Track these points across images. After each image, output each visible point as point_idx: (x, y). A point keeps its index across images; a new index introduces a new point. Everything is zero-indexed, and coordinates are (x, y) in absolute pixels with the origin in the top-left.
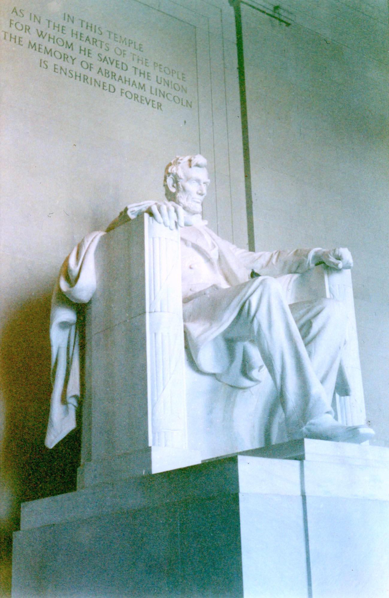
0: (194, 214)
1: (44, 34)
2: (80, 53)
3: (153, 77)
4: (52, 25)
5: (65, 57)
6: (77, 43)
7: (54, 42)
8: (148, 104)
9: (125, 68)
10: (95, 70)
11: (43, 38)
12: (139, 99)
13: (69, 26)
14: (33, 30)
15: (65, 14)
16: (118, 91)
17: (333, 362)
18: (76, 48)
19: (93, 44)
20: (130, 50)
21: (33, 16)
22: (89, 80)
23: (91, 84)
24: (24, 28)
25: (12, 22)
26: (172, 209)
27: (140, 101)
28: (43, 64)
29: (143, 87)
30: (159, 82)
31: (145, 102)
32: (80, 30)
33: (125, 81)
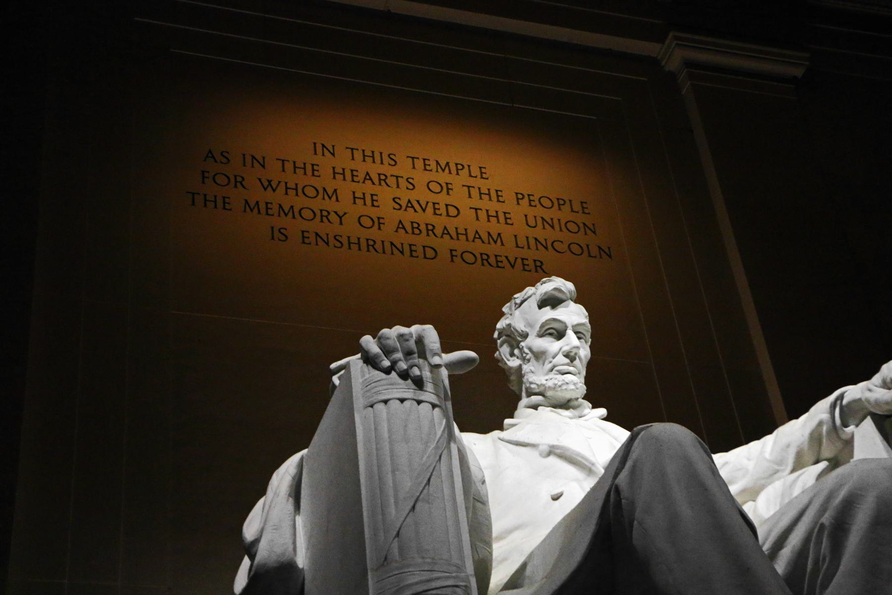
1: (274, 184)
2: (355, 203)
5: (325, 216)
6: (345, 189)
7: (297, 195)
8: (513, 267)
11: (274, 191)
12: (492, 260)
13: (326, 163)
15: (315, 144)
16: (444, 254)
19: (380, 184)
20: (458, 181)
21: (249, 160)
22: (378, 246)
23: (384, 252)
24: (233, 180)
25: (206, 175)
27: (495, 265)
30: (532, 223)
32: (349, 165)
33: (458, 234)
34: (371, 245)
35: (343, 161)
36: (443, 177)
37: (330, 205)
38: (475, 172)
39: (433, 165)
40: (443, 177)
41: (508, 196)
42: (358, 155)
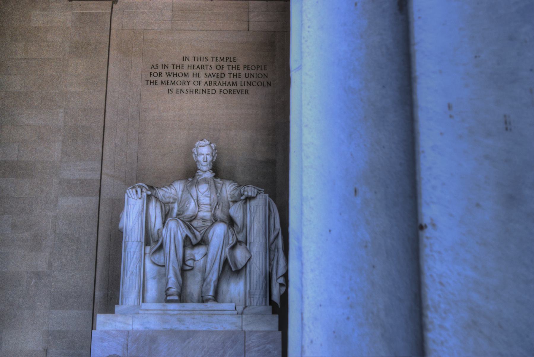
0: (206, 171)
3: (242, 75)
4: (175, 66)
5: (183, 83)
6: (191, 72)
9: (223, 75)
10: (203, 83)
12: (232, 92)
13: (186, 63)
14: (164, 74)
16: (218, 91)
17: (217, 254)
18: (191, 75)
21: (164, 66)
22: (198, 92)
26: (134, 191)
28: (170, 91)
29: (235, 84)
30: (247, 76)
31: (236, 92)
34: (196, 91)
35: (191, 62)
36: (222, 63)
37: (185, 79)
38: (232, 60)
39: (219, 59)
40: (222, 63)
41: (241, 67)
42: (196, 59)
